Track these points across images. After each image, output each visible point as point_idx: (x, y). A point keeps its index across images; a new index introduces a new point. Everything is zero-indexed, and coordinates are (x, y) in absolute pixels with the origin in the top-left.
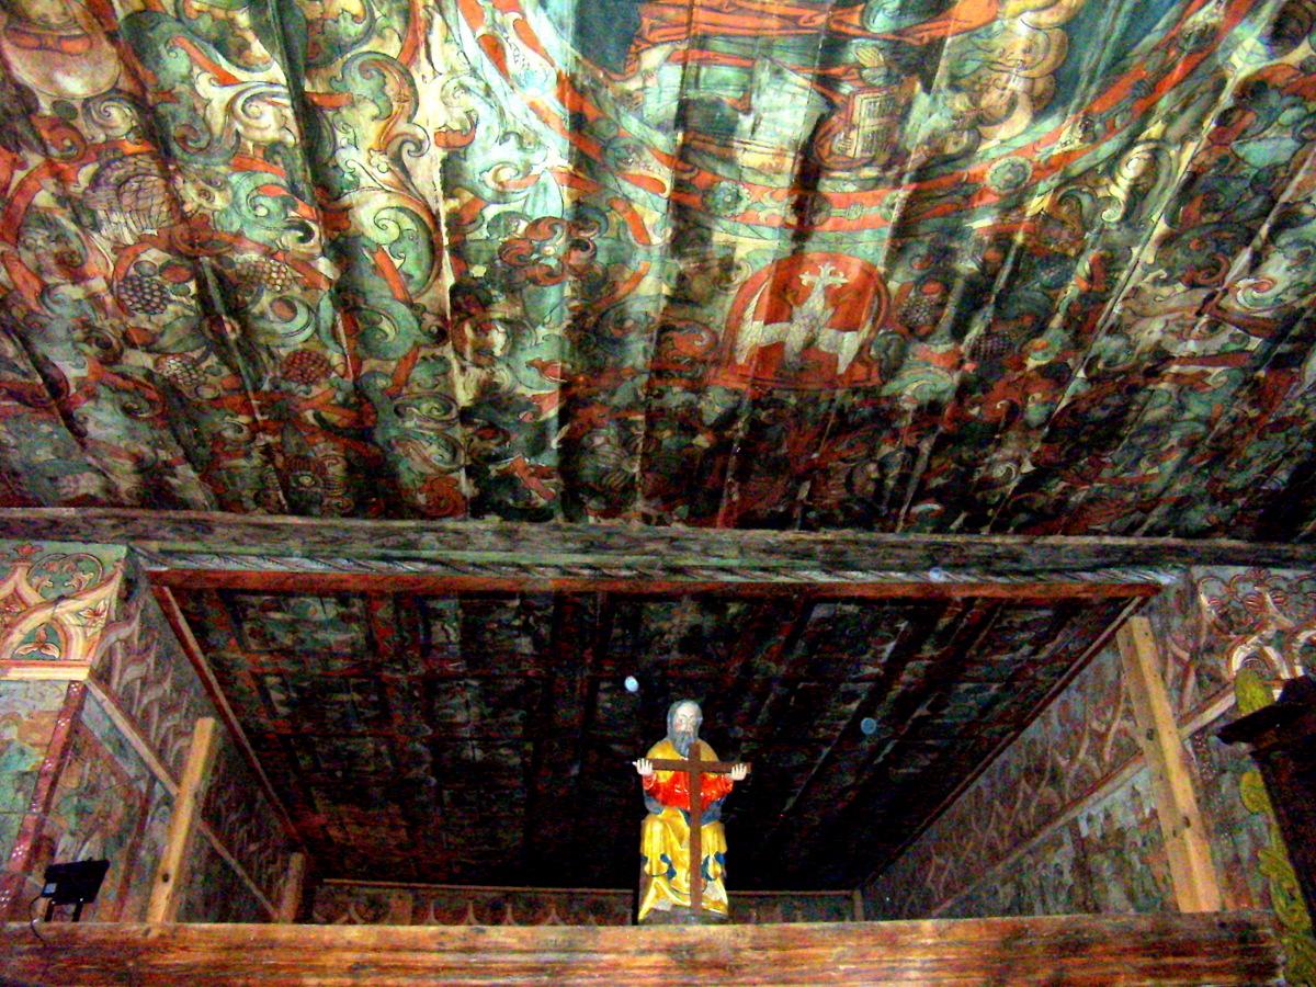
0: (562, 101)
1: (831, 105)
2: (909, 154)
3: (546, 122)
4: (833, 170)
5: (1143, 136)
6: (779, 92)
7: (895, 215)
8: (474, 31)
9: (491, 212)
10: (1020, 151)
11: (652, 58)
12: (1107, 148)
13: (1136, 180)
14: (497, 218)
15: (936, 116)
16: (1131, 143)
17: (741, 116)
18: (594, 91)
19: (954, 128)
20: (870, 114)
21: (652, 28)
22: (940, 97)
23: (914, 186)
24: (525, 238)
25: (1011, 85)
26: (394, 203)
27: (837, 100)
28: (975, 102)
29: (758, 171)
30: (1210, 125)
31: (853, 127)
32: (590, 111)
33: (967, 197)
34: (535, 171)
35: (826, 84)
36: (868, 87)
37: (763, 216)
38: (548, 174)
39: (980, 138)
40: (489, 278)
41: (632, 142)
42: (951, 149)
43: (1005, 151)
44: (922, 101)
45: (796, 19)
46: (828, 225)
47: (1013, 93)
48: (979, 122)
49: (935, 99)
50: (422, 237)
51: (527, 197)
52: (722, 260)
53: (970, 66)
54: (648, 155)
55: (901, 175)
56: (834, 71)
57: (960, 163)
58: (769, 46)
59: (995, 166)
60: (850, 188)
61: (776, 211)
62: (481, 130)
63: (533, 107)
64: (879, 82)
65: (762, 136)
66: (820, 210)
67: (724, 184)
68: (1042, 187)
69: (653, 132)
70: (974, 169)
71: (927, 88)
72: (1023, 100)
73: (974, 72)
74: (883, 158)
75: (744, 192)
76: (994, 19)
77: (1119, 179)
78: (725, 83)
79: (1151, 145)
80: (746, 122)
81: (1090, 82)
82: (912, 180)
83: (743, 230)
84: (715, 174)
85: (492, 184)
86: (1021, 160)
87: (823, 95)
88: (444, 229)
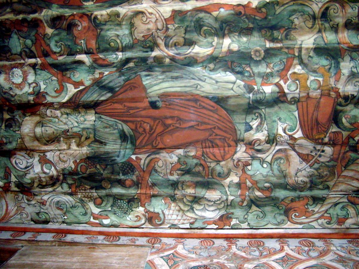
30: (20, 17)
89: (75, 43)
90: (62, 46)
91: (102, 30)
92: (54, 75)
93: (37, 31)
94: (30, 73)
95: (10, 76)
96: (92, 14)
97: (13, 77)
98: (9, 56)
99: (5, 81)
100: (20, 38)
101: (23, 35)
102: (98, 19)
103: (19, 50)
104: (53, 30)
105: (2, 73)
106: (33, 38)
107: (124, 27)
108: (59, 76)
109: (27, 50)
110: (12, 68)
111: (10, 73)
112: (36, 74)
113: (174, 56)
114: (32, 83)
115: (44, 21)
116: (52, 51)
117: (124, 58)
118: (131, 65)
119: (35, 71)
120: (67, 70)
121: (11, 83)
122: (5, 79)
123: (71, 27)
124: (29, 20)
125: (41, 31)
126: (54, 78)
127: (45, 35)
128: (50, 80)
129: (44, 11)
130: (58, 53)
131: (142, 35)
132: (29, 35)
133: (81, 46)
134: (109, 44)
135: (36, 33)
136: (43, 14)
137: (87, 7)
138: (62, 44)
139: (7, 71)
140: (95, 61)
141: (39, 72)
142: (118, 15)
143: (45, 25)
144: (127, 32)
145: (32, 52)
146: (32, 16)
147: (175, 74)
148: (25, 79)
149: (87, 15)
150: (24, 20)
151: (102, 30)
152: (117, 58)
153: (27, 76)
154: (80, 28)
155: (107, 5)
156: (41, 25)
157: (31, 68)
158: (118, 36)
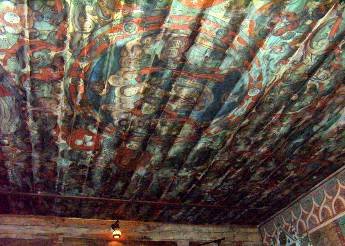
0: (252, 66)
1: (183, 54)
2: (162, 38)
3: (259, 62)
4: (186, 37)
5: (89, 35)
6: (196, 60)
7: (168, 19)
8: (262, 83)
9: (290, 41)
10: (128, 36)
11: (225, 72)
12: (99, 32)
13: (85, 21)
14: (289, 39)
15: (154, 48)
16: (92, 33)
17: (208, 56)
18: (243, 66)
19: (149, 45)
20: (173, 51)
21: (222, 78)
22: (153, 53)
23: (161, 28)
24: (286, 30)
25: (133, 55)
26: (313, 50)
27: (181, 56)
28: (143, 51)
29: (208, 40)
30: (69, 36)
31: (178, 49)
32: (246, 62)
33: (143, 22)
34: (269, 50)
35: (184, 60)
36: (173, 59)
37: (211, 25)
38: (267, 49)
39: (141, 41)
40: (308, 18)
41: (240, 53)
42: (150, 39)
43: (133, 36)
44: (158, 52)
45: (189, 75)
46: (190, 19)
47: (132, 53)
48: (141, 46)
49: (155, 52)
50: (314, 39)
51: (277, 43)
52: (230, 12)
53: (145, 60)
54: (237, 49)
55: (165, 32)
56: (181, 62)
57: (146, 34)
58: (196, 70)
59: (135, 32)
60: (182, 31)
61: (206, 26)
62: (275, 63)
63: (259, 65)
64: (170, 59)
65: (204, 49)
66: (193, 24)
67: (219, 38)
68: (118, 22)
69: (234, 55)
70: (142, 32)
71: (156, 56)
72: (129, 51)
73: (144, 59)
74: (170, 39)
75: (214, 34)
76: (140, 70)
77: (91, 21)
78: (210, 64)
79: (85, 32)
80: (207, 54)
81: (110, 52)
82: (162, 30)
83: (219, 21)
84: (221, 41)
85: (283, 48)
86: (127, 33)
87: (185, 57)
88: (307, 38)
89: (39, 68)
90: (38, 59)
91: (49, 84)
92: (13, 47)
93: (54, 46)
94: (15, 30)
95: (12, 13)
96: (62, 80)
97: (11, 15)
98: (32, 18)
99: (6, 6)
100: (49, 32)
101: (52, 35)
102: (57, 83)
103: (38, 28)
104: (53, 56)
105: (16, 7)
106: (48, 42)
107: (49, 95)
108: (12, 51)
109: (37, 34)
110: (21, 17)
111: (15, 14)
112: (14, 34)
113: (27, 111)
114: (5, 30)
115: (62, 52)
116: (35, 52)
117: (26, 90)
118: (21, 93)
119: (17, 34)
120: (18, 57)
121: (5, 12)
122: (8, 8)
123: (54, 67)
124: (65, 42)
125: (54, 48)
126: (10, 47)
127: (50, 50)
128: (8, 44)
129: (71, 54)
130: (33, 55)
131: (42, 102)
132: (51, 39)
133: (37, 71)
134: (37, 86)
135: (52, 45)
136: (68, 52)
137: (67, 79)
138: (40, 59)
139: (17, 11)
140: (25, 75)
141: (16, 37)
142: (59, 92)
143: (58, 52)
144: (45, 95)
145: (35, 38)
146: (68, 45)
147: (14, 111)
148: (9, 25)
149: (62, 78)
150: (65, 38)
151: (49, 84)
152: (27, 86)
153: (12, 26)
154: (52, 72)
155: (67, 89)
156: (59, 49)
157: (20, 32)
158: (43, 91)
